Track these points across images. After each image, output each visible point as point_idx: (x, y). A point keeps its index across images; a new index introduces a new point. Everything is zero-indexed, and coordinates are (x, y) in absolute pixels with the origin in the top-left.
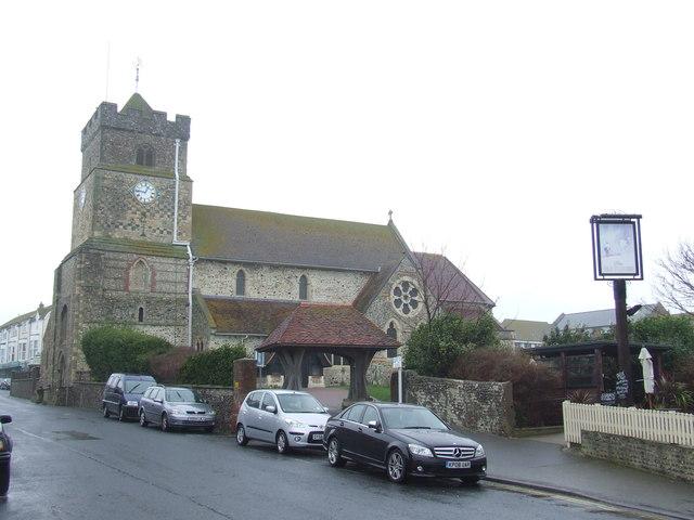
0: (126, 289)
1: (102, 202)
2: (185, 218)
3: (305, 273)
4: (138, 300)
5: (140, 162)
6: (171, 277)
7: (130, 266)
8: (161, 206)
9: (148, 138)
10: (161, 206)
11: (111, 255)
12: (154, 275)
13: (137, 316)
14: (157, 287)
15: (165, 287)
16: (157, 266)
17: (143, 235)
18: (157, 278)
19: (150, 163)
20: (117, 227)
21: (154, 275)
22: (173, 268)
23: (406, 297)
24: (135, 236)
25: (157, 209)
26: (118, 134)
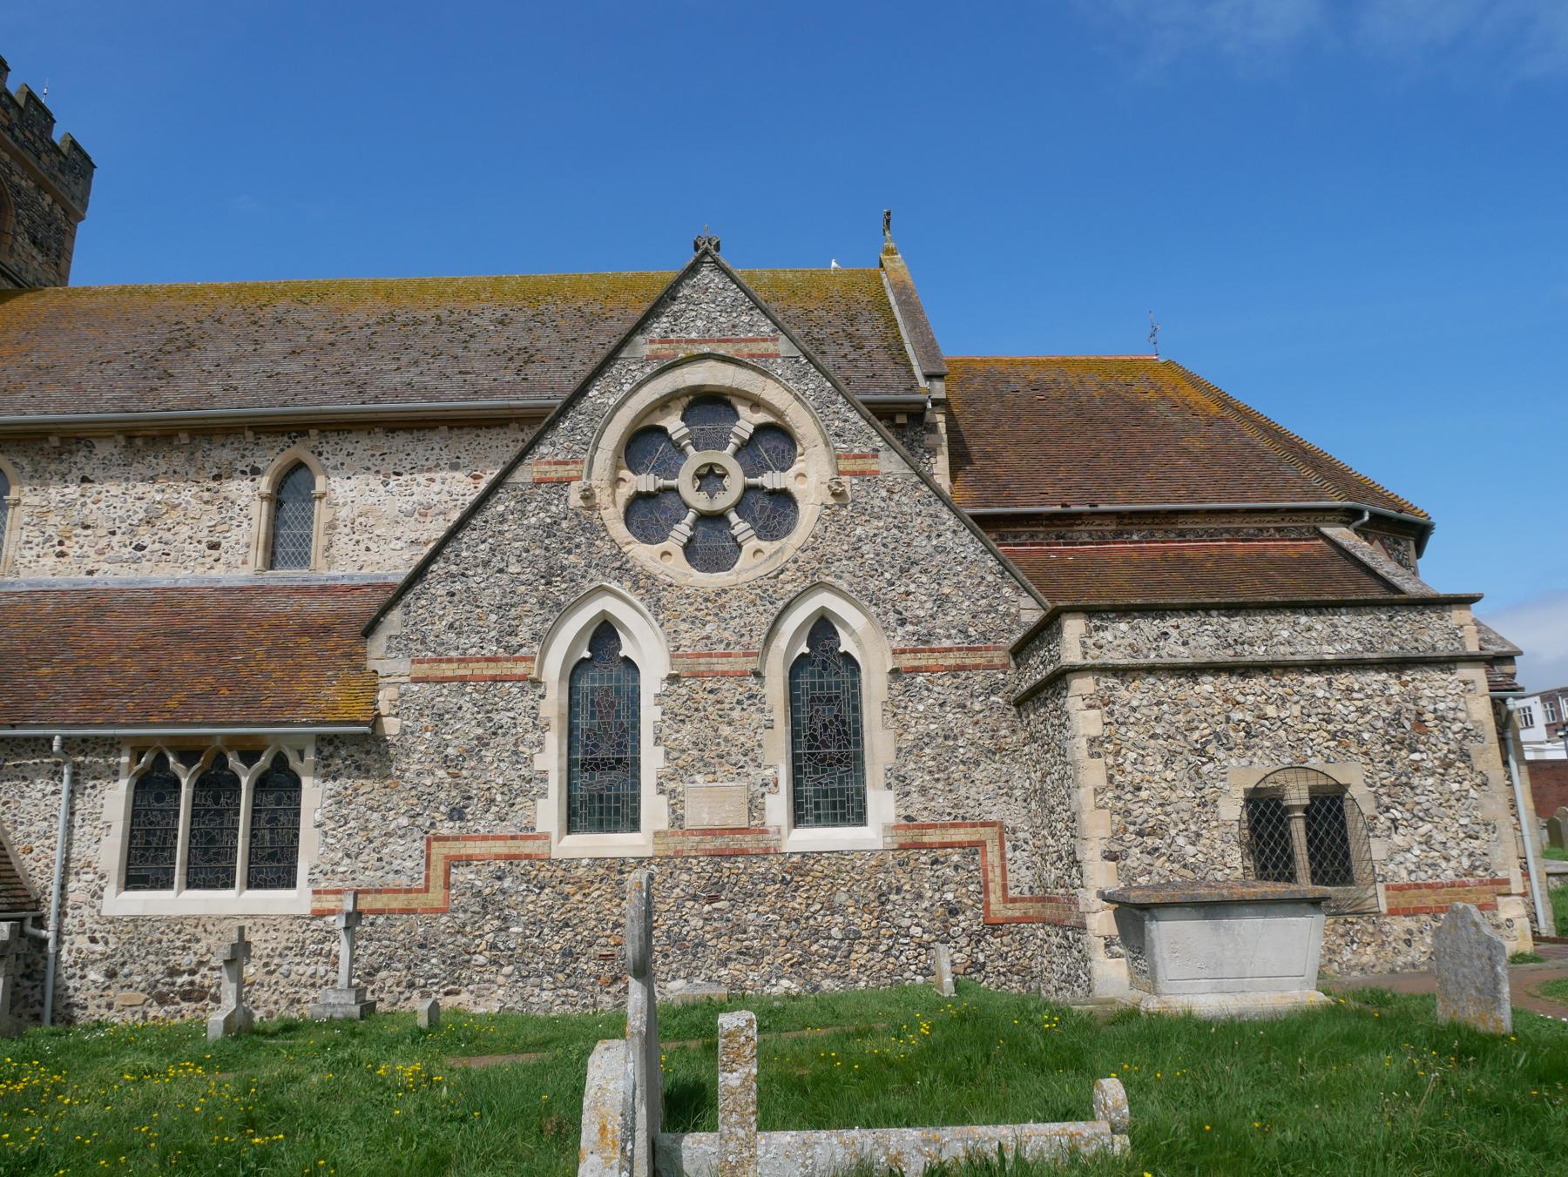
3: (299, 450)
23: (709, 477)
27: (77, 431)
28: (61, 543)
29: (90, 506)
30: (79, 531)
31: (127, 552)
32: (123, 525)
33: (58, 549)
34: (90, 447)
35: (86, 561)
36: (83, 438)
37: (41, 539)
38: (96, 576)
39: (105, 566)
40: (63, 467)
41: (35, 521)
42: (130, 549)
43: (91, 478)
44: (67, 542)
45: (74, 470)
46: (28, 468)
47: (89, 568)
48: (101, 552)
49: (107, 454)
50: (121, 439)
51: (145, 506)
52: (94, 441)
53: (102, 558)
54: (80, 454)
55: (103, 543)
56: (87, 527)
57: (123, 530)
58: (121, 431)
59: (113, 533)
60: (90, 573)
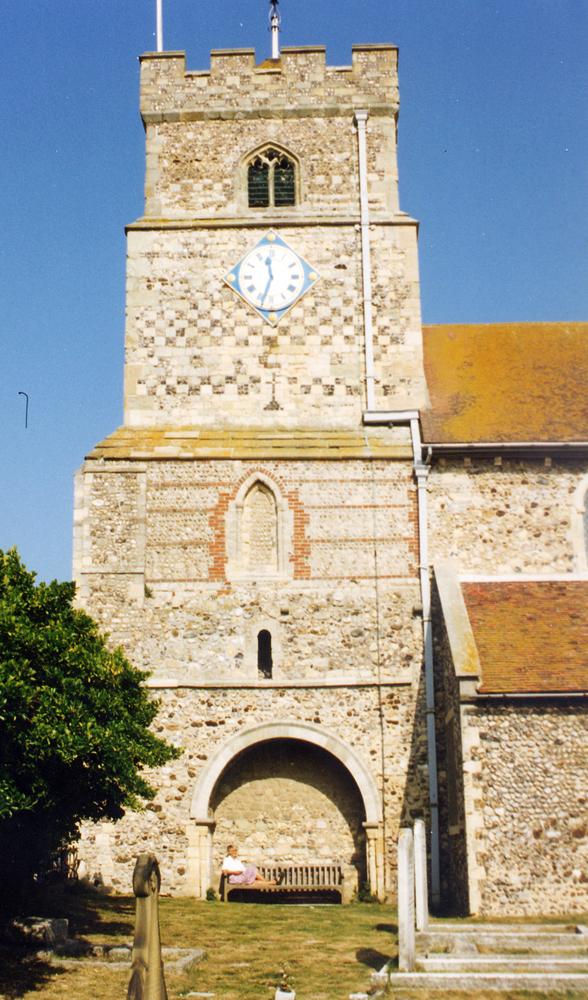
0: (217, 571)
1: (149, 324)
5: (257, 198)
7: (225, 500)
9: (273, 130)
10: (324, 311)
12: (301, 521)
13: (252, 658)
14: (315, 561)
15: (346, 560)
16: (309, 495)
17: (274, 406)
18: (312, 531)
20: (195, 390)
21: (301, 521)
22: (361, 495)
24: (243, 412)
25: (310, 321)
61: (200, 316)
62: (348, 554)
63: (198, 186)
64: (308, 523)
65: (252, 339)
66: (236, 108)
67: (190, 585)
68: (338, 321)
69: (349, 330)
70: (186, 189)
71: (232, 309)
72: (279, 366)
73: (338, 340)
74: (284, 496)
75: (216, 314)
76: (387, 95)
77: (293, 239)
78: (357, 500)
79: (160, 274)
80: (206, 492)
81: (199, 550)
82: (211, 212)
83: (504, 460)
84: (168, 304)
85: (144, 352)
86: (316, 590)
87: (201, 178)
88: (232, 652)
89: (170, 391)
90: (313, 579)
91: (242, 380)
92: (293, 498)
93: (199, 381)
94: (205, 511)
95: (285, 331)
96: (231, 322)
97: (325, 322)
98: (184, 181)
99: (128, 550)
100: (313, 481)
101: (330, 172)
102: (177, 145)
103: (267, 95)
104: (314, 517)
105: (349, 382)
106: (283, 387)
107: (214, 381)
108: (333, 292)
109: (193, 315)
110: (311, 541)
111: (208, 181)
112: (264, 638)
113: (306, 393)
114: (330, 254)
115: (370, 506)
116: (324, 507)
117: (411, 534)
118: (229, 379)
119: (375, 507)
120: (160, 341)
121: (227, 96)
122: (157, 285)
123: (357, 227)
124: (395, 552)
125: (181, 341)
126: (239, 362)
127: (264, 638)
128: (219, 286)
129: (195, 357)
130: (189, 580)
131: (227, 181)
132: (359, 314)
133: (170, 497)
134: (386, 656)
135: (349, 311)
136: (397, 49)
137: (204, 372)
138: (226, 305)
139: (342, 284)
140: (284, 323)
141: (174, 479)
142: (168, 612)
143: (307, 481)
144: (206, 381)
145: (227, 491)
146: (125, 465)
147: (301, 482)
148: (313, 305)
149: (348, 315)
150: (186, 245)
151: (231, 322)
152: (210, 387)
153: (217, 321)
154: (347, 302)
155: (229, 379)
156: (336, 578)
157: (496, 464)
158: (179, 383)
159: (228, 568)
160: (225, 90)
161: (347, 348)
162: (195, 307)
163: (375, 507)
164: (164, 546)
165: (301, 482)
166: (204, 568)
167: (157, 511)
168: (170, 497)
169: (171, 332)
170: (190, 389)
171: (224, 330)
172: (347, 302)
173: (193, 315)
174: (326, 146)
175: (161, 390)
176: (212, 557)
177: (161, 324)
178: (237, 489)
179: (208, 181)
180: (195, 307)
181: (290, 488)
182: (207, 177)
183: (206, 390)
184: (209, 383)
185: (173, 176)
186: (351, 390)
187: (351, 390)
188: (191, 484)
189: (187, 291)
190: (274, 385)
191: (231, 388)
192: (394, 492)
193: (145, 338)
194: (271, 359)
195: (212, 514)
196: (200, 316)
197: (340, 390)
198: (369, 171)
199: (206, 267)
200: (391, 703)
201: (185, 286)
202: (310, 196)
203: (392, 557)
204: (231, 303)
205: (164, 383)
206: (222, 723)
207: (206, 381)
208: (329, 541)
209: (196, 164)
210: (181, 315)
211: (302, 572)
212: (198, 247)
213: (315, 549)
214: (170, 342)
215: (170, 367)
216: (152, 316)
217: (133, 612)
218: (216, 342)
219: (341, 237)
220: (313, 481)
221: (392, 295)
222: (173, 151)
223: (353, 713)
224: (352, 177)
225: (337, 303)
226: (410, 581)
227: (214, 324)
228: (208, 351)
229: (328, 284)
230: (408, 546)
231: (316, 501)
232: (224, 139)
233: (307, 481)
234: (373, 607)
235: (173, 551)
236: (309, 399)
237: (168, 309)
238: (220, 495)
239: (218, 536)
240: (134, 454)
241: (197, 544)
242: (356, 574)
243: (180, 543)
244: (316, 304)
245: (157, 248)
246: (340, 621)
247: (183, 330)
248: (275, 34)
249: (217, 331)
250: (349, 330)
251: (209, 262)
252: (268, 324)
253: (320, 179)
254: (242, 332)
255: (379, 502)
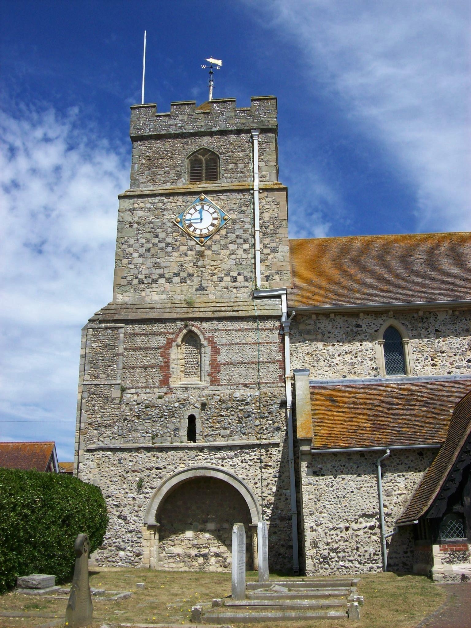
0: (165, 381)
1: (130, 246)
2: (274, 250)
4: (183, 403)
5: (195, 177)
6: (249, 354)
7: (169, 342)
8: (232, 236)
10: (232, 236)
11: (138, 328)
12: (215, 353)
13: (184, 432)
14: (223, 376)
16: (222, 338)
17: (201, 288)
18: (222, 358)
19: (213, 176)
20: (155, 281)
21: (215, 353)
22: (251, 337)
26: (157, 145)
27: (431, 309)
28: (432, 360)
29: (442, 342)
30: (439, 354)
31: (464, 363)
32: (459, 351)
33: (432, 362)
34: (436, 315)
35: (446, 368)
36: (432, 312)
37: (423, 359)
38: (452, 374)
39: (456, 370)
40: (426, 325)
41: (419, 350)
42: (465, 362)
43: (439, 330)
44: (435, 359)
45: (431, 327)
46: (409, 326)
47: (448, 371)
48: (452, 364)
49: (444, 319)
50: (450, 312)
51: (467, 343)
52: (437, 313)
53: (453, 366)
54: (431, 319)
55: (452, 360)
56: (443, 352)
57: (460, 353)
58: (450, 308)
59: (455, 355)
60: (449, 373)
61: (159, 241)
62: (242, 370)
63: (161, 172)
64: (219, 353)
65: (189, 253)
66: (184, 131)
67: (148, 390)
68: (240, 241)
69: (246, 246)
70: (155, 174)
71: (178, 237)
72: (204, 266)
73: (240, 252)
74: (205, 339)
75: (169, 240)
76: (270, 122)
77: (215, 198)
78: (249, 340)
79: (136, 219)
80: (159, 338)
81: (154, 370)
82: (168, 186)
83: (335, 316)
84: (141, 236)
85: (125, 261)
86: (225, 392)
87: (163, 168)
88: (172, 427)
89: (141, 282)
90: (222, 385)
91: (183, 275)
92: (210, 340)
93: (158, 276)
94: (158, 348)
95: (209, 248)
96: (178, 243)
97: (232, 242)
98: (152, 170)
99: (111, 371)
100: (223, 330)
101: (238, 162)
102: (150, 151)
103: (202, 124)
104: (223, 350)
105: (246, 274)
106: (207, 277)
107: (167, 276)
108: (237, 226)
109: (156, 240)
110: (221, 364)
111: (166, 169)
112: (192, 419)
113: (220, 281)
114: (236, 206)
115: (256, 343)
116: (229, 345)
117: (281, 358)
118: (176, 275)
119: (258, 344)
120: (136, 255)
121: (179, 125)
122: (136, 226)
123: (252, 192)
124: (271, 369)
125: (149, 255)
126: (182, 266)
127: (192, 419)
128: (171, 225)
129: (156, 264)
130: (148, 388)
131: (178, 169)
132: (251, 238)
133: (139, 341)
134: (264, 428)
135: (246, 236)
136: (276, 99)
137: (160, 271)
138: (175, 234)
139: (242, 222)
140: (209, 243)
141: (140, 331)
142: (134, 405)
143: (219, 330)
144: (162, 276)
145: (172, 336)
146: (112, 325)
147: (216, 331)
148: (225, 233)
149: (246, 238)
150: (152, 204)
151: (178, 243)
152: (164, 279)
153: (169, 244)
154: (245, 231)
155: (176, 275)
156: (235, 384)
157: (331, 317)
158: (146, 278)
159: (171, 380)
160: (178, 122)
161: (244, 256)
162: (157, 236)
163: (258, 344)
164: (133, 368)
165: (216, 331)
166: (157, 379)
167: (130, 349)
168: (139, 341)
169: (142, 250)
170: (153, 280)
171: (173, 248)
172: (245, 231)
173: (156, 240)
174: (236, 149)
175: (135, 281)
176: (162, 374)
177: (136, 246)
178: (178, 335)
179: (166, 169)
180: (157, 236)
181: (208, 334)
182: (166, 167)
183: (162, 281)
184: (164, 278)
185: (147, 167)
186: (246, 279)
187: (246, 279)
188: (150, 334)
189: (152, 228)
190: (202, 277)
191: (176, 280)
192: (270, 335)
193: (127, 254)
194: (200, 263)
195: (162, 350)
196: (159, 241)
197: (240, 279)
198: (259, 161)
199: (164, 215)
200: (267, 455)
201: (152, 225)
202: (226, 175)
203: (269, 372)
204: (178, 234)
205: (137, 278)
206: (165, 468)
207: (162, 276)
208: (232, 364)
209: (161, 160)
210: (148, 241)
211: (215, 381)
212: (160, 205)
213: (222, 368)
214: (141, 255)
215: (141, 269)
216: (132, 242)
217: (113, 406)
218: (168, 254)
219: (242, 197)
220: (223, 330)
221: (272, 227)
222: (148, 154)
223: (244, 461)
224: (250, 164)
225: (239, 232)
226: (279, 385)
227: (168, 245)
228: (162, 261)
229: (234, 222)
230: (278, 365)
231: (224, 341)
232: (177, 147)
233: (219, 330)
234: (257, 401)
235: (138, 371)
236: (223, 284)
237: (141, 238)
238: (167, 339)
239: (165, 362)
240: (117, 317)
241: (153, 367)
242: (247, 382)
243: (143, 367)
244: (227, 233)
245: (136, 206)
246: (237, 409)
247: (150, 248)
248: (212, 88)
249: (169, 249)
250: (246, 246)
251: (165, 213)
252: (199, 244)
253: (231, 166)
254: (184, 248)
255: (261, 340)
